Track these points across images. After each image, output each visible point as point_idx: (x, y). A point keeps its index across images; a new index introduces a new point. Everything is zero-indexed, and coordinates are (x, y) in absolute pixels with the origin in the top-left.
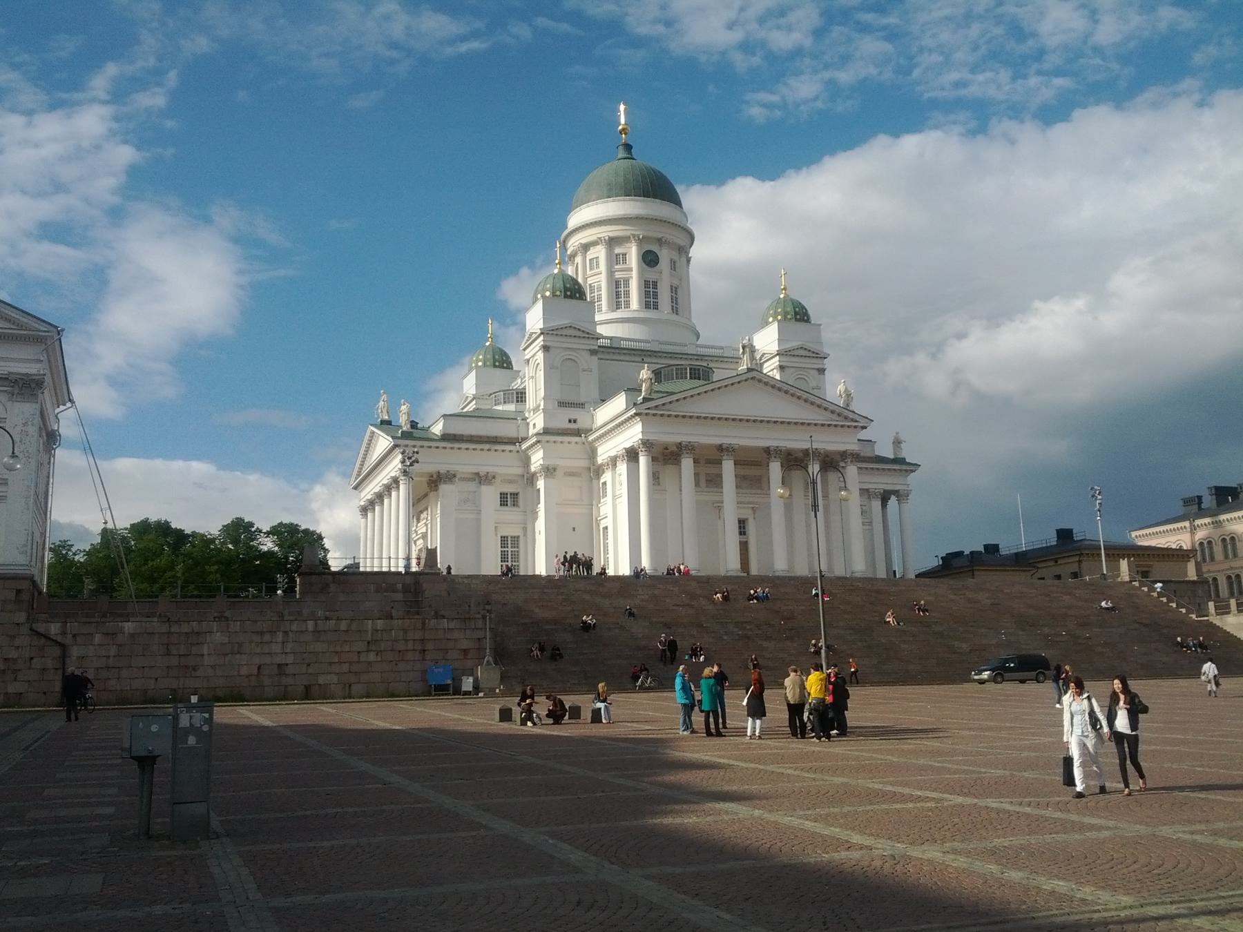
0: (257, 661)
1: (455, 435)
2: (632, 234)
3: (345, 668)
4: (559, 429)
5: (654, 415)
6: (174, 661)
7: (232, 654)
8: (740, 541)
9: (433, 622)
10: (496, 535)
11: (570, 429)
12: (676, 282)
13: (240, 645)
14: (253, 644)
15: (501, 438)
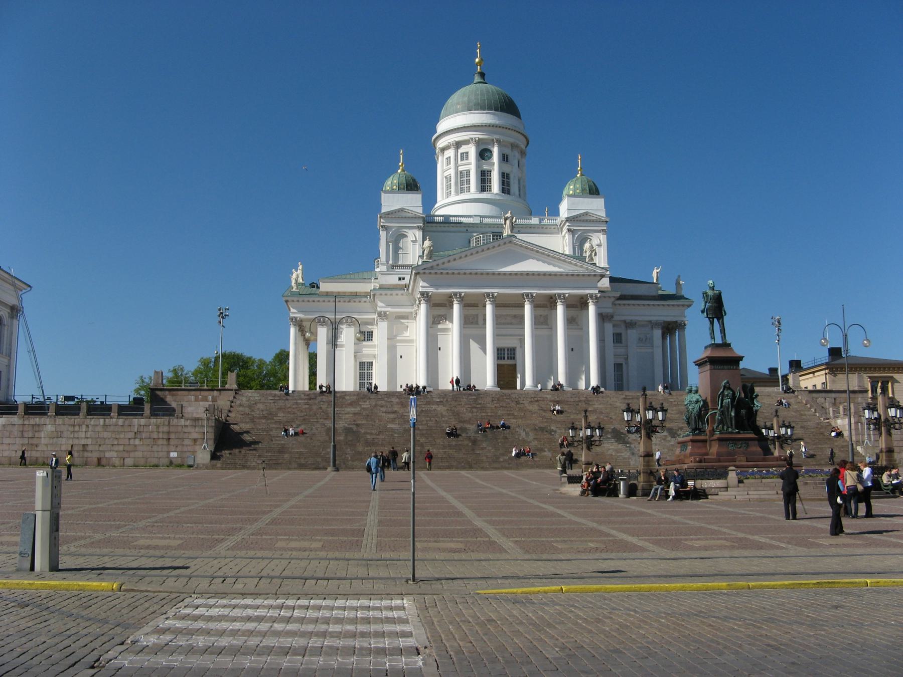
0: (71, 442)
1: (327, 292)
2: (472, 139)
3: (121, 448)
4: (390, 285)
5: (430, 273)
6: (26, 441)
7: (57, 437)
8: (497, 365)
9: (175, 420)
10: (356, 361)
11: (399, 285)
12: (507, 169)
13: (62, 432)
14: (69, 432)
15: (360, 293)
